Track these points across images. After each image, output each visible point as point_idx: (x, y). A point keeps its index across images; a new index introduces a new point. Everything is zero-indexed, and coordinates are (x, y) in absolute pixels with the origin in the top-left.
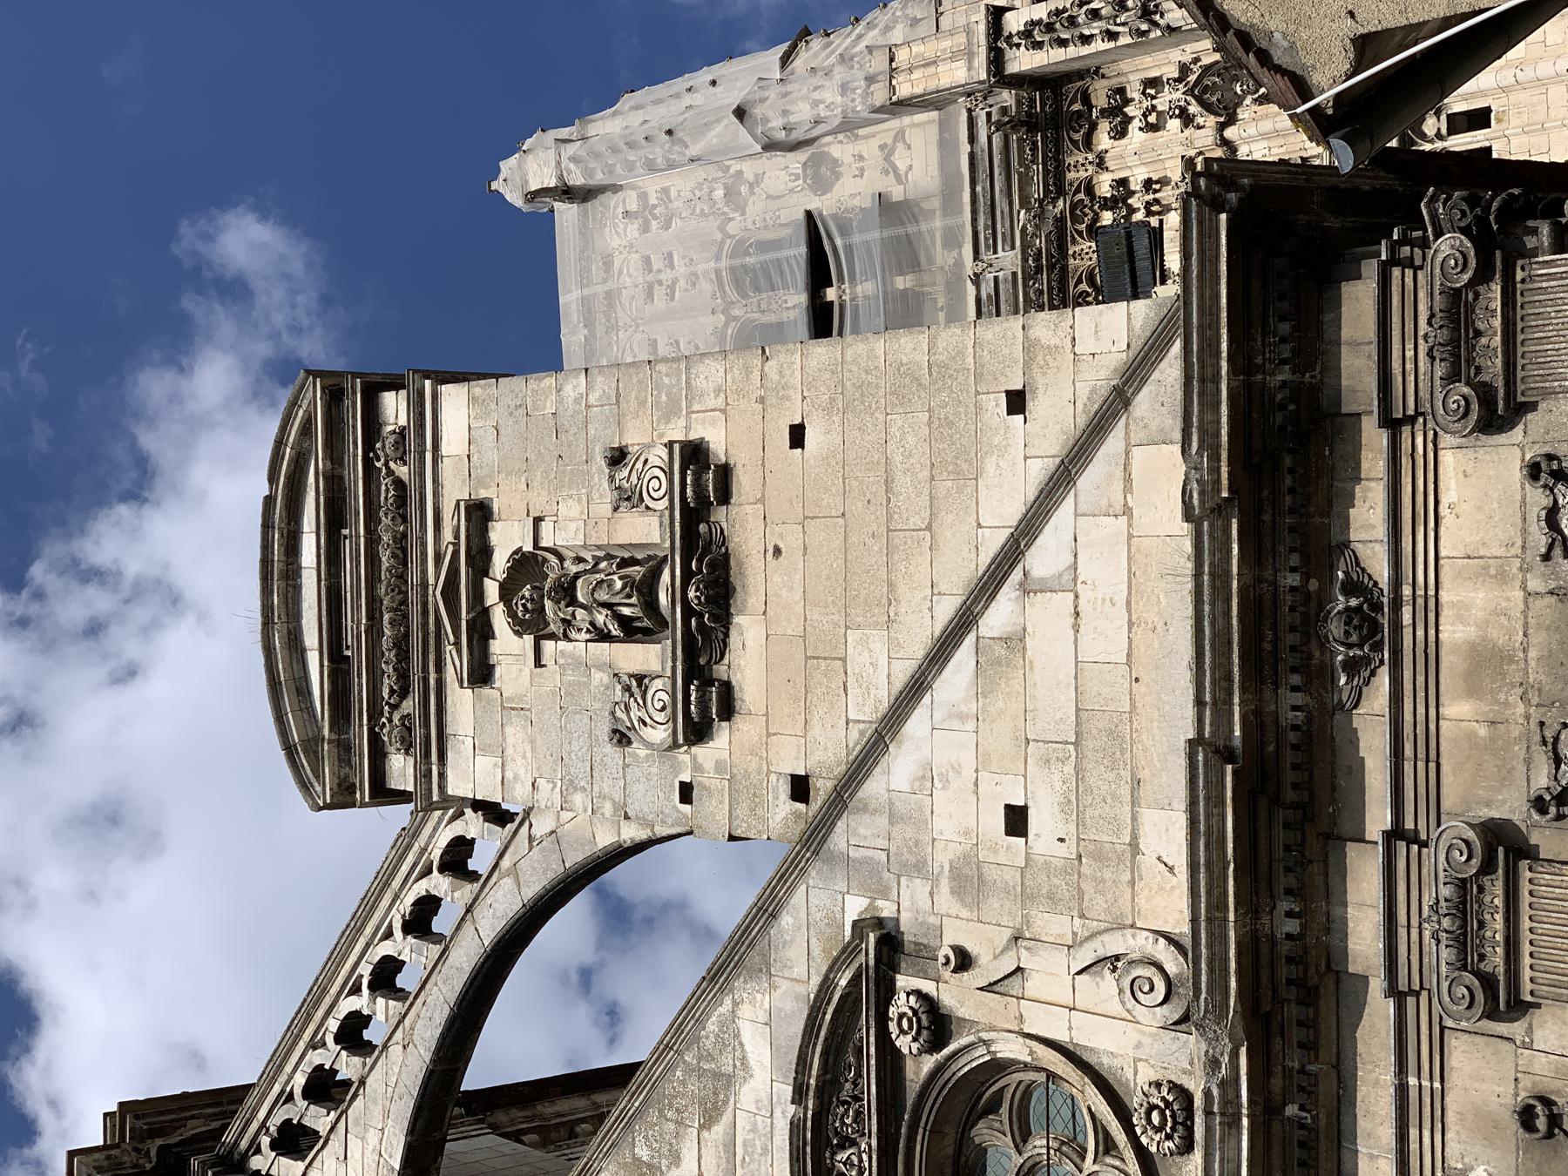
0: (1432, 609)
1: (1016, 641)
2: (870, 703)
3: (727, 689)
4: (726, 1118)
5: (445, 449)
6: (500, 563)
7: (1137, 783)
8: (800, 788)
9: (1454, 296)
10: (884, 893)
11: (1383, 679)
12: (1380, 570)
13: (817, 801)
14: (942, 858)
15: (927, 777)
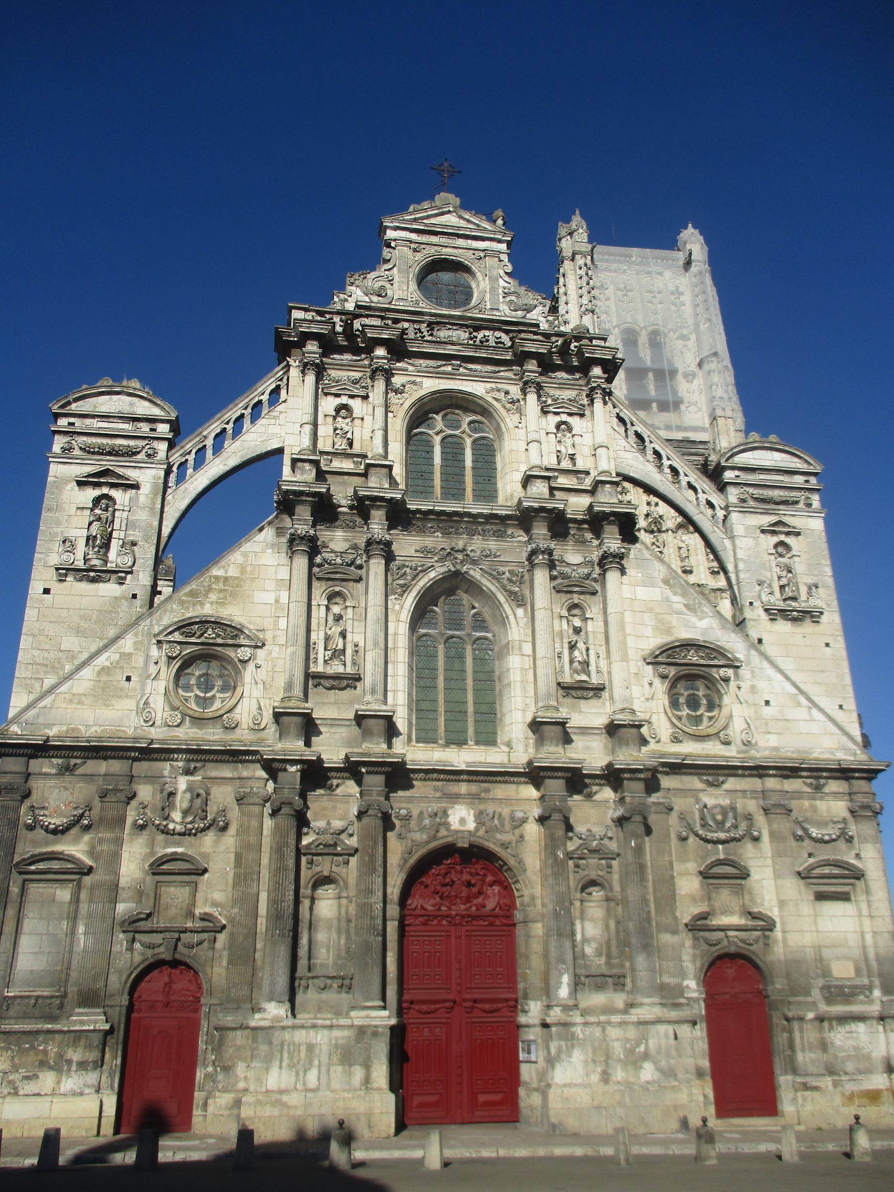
0: (822, 799)
1: (799, 704)
2: (779, 661)
3: (776, 620)
4: (688, 612)
5: (809, 519)
6: (789, 540)
7: (780, 734)
8: (760, 641)
9: (869, 807)
10: (746, 665)
11: (810, 790)
12: (826, 790)
13: (757, 645)
14: (755, 683)
15: (770, 679)
